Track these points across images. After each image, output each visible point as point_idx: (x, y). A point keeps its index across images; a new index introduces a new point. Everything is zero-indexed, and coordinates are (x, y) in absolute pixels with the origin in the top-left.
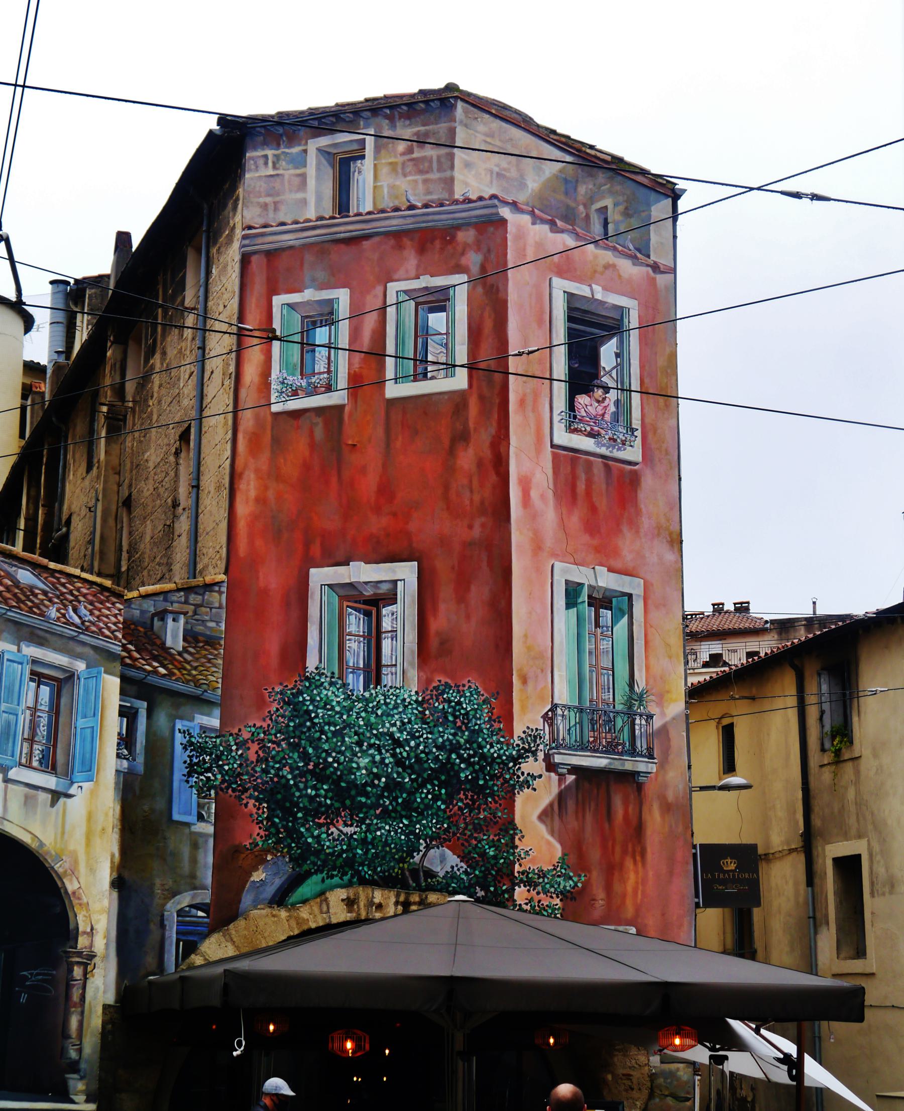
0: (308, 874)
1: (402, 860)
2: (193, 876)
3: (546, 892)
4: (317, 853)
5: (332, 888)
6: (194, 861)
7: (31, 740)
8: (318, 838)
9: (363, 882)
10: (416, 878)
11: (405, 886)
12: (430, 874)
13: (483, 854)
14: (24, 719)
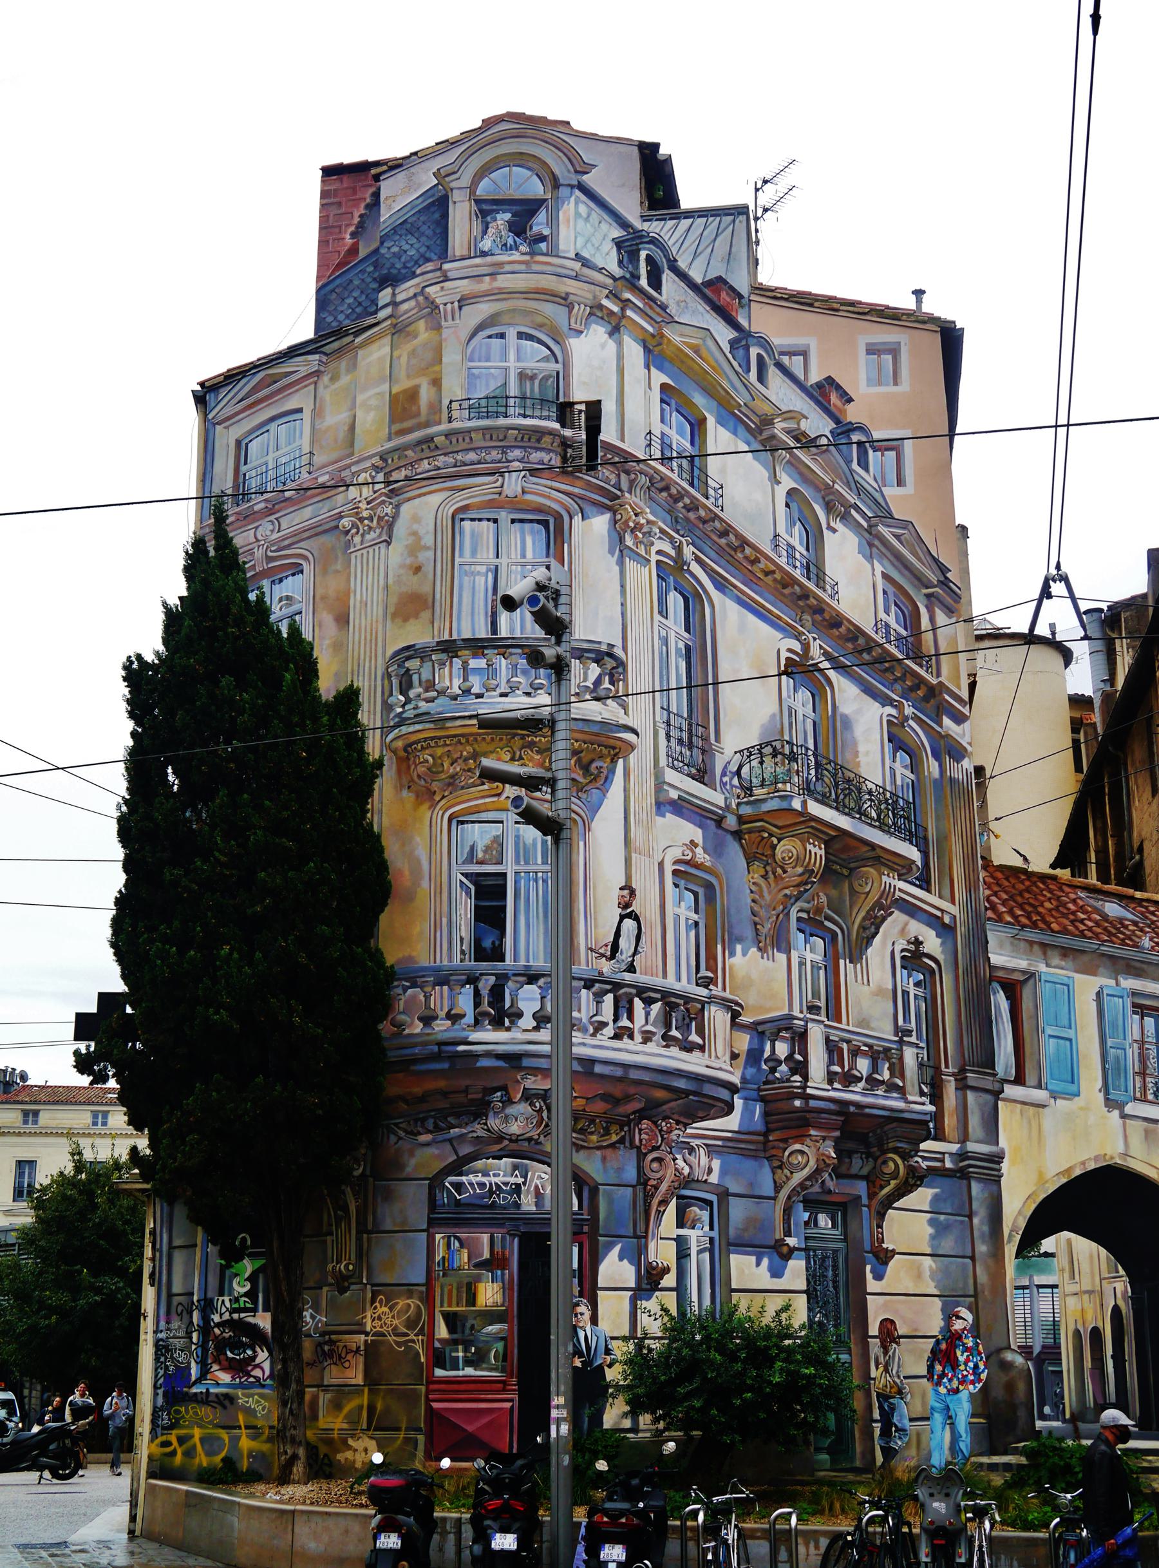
7: (1143, 1073)
14: (1132, 1052)
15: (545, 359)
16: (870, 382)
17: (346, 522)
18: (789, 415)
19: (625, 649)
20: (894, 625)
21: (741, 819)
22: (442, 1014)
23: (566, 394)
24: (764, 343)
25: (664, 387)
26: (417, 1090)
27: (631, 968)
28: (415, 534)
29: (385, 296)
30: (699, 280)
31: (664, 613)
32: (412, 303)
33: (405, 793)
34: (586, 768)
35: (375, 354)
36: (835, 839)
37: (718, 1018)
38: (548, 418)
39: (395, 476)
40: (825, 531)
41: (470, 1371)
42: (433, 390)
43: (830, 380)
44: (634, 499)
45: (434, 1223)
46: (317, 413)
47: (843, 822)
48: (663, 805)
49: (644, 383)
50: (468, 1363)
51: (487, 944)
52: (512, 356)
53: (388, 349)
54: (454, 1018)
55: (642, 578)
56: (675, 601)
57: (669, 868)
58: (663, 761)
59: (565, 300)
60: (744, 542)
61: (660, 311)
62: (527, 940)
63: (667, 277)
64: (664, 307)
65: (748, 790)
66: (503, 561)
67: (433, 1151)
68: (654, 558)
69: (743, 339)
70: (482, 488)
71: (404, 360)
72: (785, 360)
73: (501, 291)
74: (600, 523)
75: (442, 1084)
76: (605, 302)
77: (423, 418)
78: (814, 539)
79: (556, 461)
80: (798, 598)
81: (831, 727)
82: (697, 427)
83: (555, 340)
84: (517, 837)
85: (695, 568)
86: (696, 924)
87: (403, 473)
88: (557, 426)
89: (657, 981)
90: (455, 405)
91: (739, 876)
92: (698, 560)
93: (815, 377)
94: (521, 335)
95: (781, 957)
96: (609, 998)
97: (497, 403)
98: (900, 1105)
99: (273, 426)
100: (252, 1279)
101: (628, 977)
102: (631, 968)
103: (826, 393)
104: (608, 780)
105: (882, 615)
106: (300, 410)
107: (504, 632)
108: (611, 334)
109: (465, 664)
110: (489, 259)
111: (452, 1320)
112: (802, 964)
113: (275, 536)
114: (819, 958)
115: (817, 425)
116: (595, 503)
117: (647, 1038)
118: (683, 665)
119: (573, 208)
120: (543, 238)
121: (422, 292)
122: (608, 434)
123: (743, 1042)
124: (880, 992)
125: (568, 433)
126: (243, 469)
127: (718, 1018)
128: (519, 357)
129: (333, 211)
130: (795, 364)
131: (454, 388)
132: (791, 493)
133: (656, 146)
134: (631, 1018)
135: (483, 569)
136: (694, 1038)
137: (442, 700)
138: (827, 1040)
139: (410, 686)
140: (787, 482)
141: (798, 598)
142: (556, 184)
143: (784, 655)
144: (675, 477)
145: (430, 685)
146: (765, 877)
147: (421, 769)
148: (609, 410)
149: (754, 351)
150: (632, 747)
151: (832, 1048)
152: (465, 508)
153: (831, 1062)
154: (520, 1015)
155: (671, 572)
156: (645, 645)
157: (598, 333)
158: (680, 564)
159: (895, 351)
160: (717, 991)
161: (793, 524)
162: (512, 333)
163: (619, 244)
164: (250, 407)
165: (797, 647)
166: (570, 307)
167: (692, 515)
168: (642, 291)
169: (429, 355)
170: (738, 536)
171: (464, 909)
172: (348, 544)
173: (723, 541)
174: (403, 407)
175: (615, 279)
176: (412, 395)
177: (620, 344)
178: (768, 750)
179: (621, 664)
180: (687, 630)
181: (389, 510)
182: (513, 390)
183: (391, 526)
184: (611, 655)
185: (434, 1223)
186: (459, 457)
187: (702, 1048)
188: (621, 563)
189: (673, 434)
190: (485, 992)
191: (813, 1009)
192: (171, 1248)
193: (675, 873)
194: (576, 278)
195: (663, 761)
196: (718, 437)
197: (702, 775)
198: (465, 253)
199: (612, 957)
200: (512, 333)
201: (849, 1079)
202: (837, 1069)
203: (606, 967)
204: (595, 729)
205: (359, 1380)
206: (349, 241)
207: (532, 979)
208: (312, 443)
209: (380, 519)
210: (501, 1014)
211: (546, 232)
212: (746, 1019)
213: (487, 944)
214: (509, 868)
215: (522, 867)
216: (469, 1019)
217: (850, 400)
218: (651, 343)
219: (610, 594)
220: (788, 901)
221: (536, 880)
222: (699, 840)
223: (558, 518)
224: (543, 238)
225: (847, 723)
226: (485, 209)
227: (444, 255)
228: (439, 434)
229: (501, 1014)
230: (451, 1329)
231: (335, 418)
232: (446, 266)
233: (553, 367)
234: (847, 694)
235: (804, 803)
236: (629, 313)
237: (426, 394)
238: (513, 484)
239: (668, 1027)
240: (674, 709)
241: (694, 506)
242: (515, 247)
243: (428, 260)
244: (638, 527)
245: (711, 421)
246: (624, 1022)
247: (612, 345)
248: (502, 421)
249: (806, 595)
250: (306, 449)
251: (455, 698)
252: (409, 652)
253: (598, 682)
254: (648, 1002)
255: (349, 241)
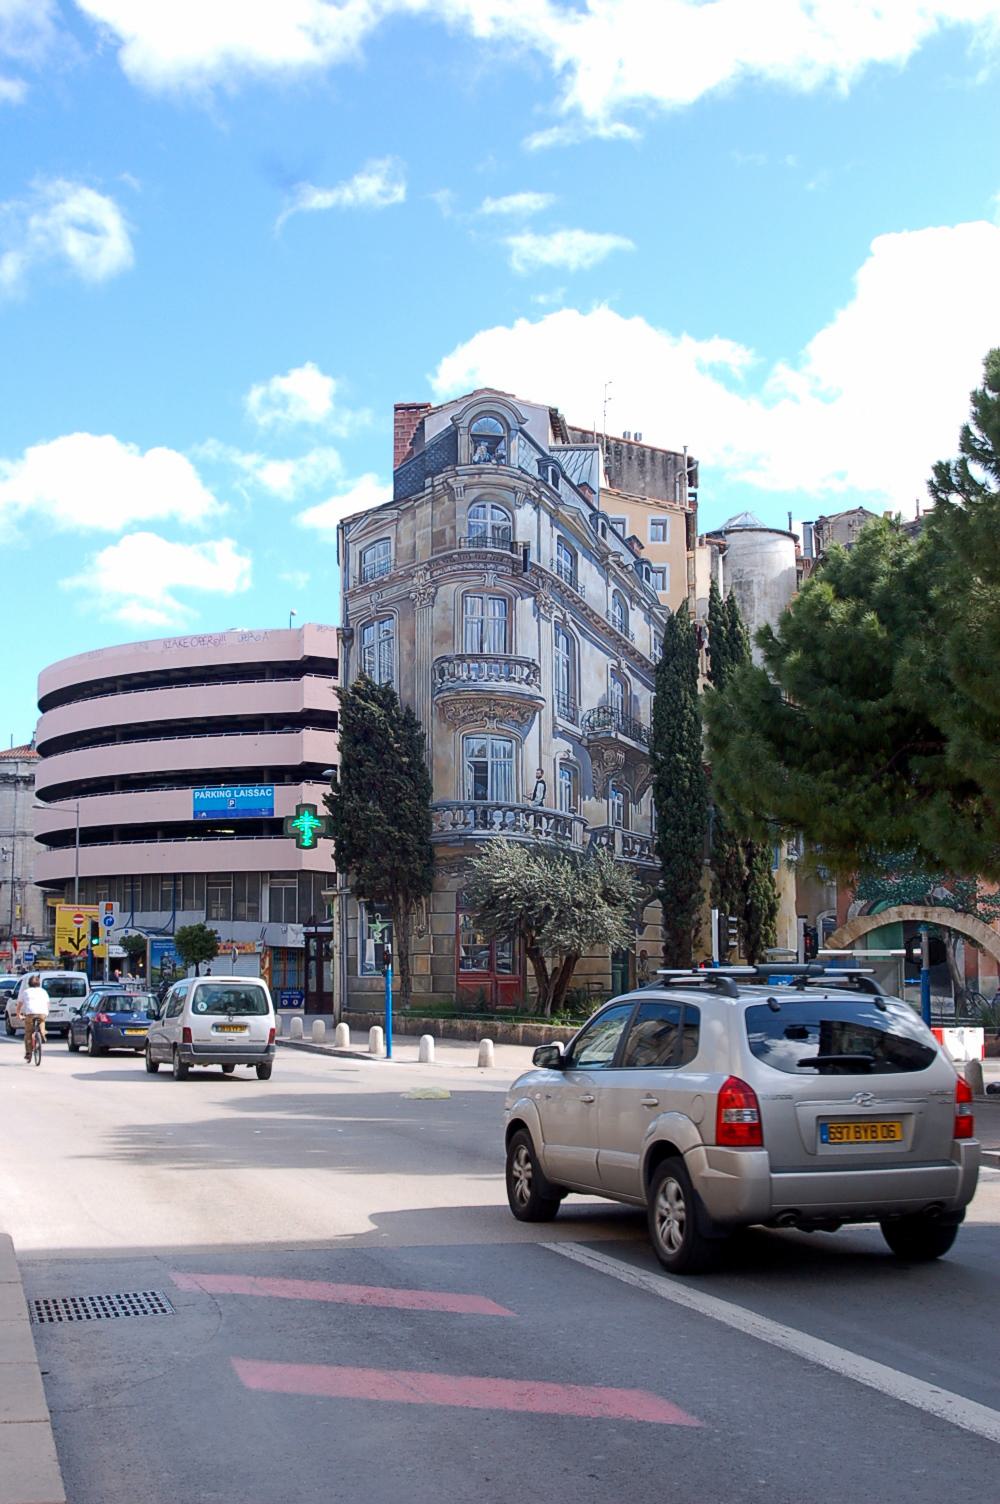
0: (880, 901)
1: (923, 893)
2: (828, 903)
3: (992, 905)
4: (883, 892)
5: (891, 906)
6: (828, 897)
8: (883, 886)
9: (905, 903)
10: (929, 901)
11: (925, 905)
12: (936, 899)
13: (961, 889)
15: (505, 520)
16: (652, 540)
17: (412, 595)
18: (618, 554)
19: (540, 661)
20: (657, 654)
21: (589, 741)
22: (460, 822)
23: (514, 538)
24: (605, 517)
25: (559, 537)
26: (451, 854)
27: (541, 804)
28: (445, 602)
29: (428, 481)
30: (576, 484)
31: (557, 645)
32: (441, 487)
33: (443, 724)
34: (522, 716)
35: (425, 512)
36: (628, 750)
37: (577, 826)
38: (506, 549)
39: (435, 573)
40: (630, 611)
41: (474, 969)
42: (452, 531)
43: (634, 537)
44: (544, 592)
45: (459, 910)
46: (398, 540)
47: (633, 743)
48: (556, 734)
49: (549, 536)
50: (474, 966)
51: (480, 792)
52: (489, 517)
53: (430, 509)
54: (466, 824)
55: (548, 628)
56: (562, 639)
57: (558, 762)
58: (556, 714)
59: (514, 490)
60: (594, 613)
61: (557, 499)
62: (496, 793)
63: (561, 480)
64: (559, 497)
65: (593, 728)
66: (485, 617)
67: (458, 880)
68: (553, 619)
69: (596, 514)
70: (476, 580)
71: (438, 516)
72: (614, 526)
73: (484, 483)
74: (529, 601)
75: (461, 852)
76: (532, 492)
77: (448, 545)
78: (625, 614)
79: (510, 570)
80: (616, 641)
81: (629, 701)
82: (574, 557)
83: (510, 510)
84: (492, 746)
85: (572, 624)
86: (569, 786)
87: (439, 572)
88: (510, 553)
89: (553, 810)
90: (462, 540)
91: (589, 767)
92: (573, 620)
93: (627, 536)
94: (493, 507)
95: (605, 801)
96: (532, 817)
97: (482, 539)
98: (652, 864)
99: (376, 545)
100: (382, 932)
101: (540, 808)
102: (541, 804)
103: (632, 543)
104: (532, 721)
105: (653, 650)
106: (389, 538)
107: (486, 652)
108: (535, 509)
109: (469, 666)
110: (478, 466)
111: (465, 948)
112: (613, 804)
113: (380, 600)
114: (620, 802)
115: (628, 559)
116: (526, 592)
117: (548, 834)
118: (565, 669)
119: (517, 442)
120: (503, 457)
121: (446, 481)
122: (533, 558)
123: (588, 836)
124: (645, 818)
125: (514, 556)
126: (363, 566)
127: (577, 826)
128: (491, 519)
129: (400, 431)
130: (619, 528)
131: (462, 531)
132: (615, 591)
133: (556, 410)
134: (541, 825)
135: (476, 620)
136: (567, 834)
137: (458, 682)
138: (623, 837)
139: (444, 675)
140: (613, 586)
141: (616, 641)
142: (509, 429)
143: (610, 667)
144: (563, 581)
145: (453, 675)
146: (599, 766)
147: (450, 714)
148: (534, 545)
149: (600, 521)
150: (543, 707)
151: (625, 840)
152: (467, 591)
153: (624, 846)
154: (494, 823)
155: (560, 627)
156: (549, 660)
157: (529, 508)
158: (564, 620)
159: (664, 524)
160: (577, 815)
161: (615, 606)
162: (489, 505)
163: (538, 461)
164: (365, 535)
165: (616, 663)
166: (516, 493)
167: (571, 600)
168: (548, 486)
169: (451, 513)
170: (590, 610)
171: (470, 776)
172: (414, 606)
173: (584, 613)
174: (437, 539)
175: (537, 481)
176: (442, 533)
177: (539, 514)
178: (601, 710)
179: (538, 668)
180: (568, 653)
181: (433, 590)
182: (489, 534)
183: (433, 598)
184: (534, 664)
185: (459, 910)
186: (465, 566)
187: (570, 839)
188: (538, 621)
189: (563, 562)
190: (479, 813)
191: (618, 824)
192: (347, 919)
193: (561, 764)
194: (519, 479)
195: (556, 714)
196: (583, 563)
197: (573, 721)
198: (466, 462)
199: (533, 799)
200: (489, 505)
201: (632, 853)
202: (626, 849)
203: (531, 804)
204: (527, 698)
205: (429, 973)
206: (409, 448)
207: (499, 808)
208: (396, 554)
209: (429, 594)
210: (487, 824)
211: (504, 454)
212: (587, 827)
213: (480, 792)
214: (489, 759)
215: (495, 760)
216: (472, 825)
217: (643, 548)
218: (554, 514)
219: (534, 636)
220: (609, 777)
221: (505, 765)
222: (571, 750)
223: (510, 599)
224: (503, 457)
225: (636, 699)
226: (476, 439)
227: (455, 462)
228: (455, 554)
229: (487, 824)
230: (467, 953)
231: (406, 542)
232: (457, 468)
233: (507, 523)
234: (637, 687)
235: (616, 735)
236: (543, 498)
237: (449, 533)
238: (490, 579)
239: (557, 830)
240: (561, 690)
241: (572, 596)
242: (489, 461)
243: (449, 465)
244: (546, 604)
245: (580, 555)
246: (538, 827)
247: (535, 514)
248: (484, 549)
249: (620, 639)
250: (393, 558)
251: (464, 681)
252: (445, 659)
253: (528, 676)
254: (548, 819)
255: (409, 448)
